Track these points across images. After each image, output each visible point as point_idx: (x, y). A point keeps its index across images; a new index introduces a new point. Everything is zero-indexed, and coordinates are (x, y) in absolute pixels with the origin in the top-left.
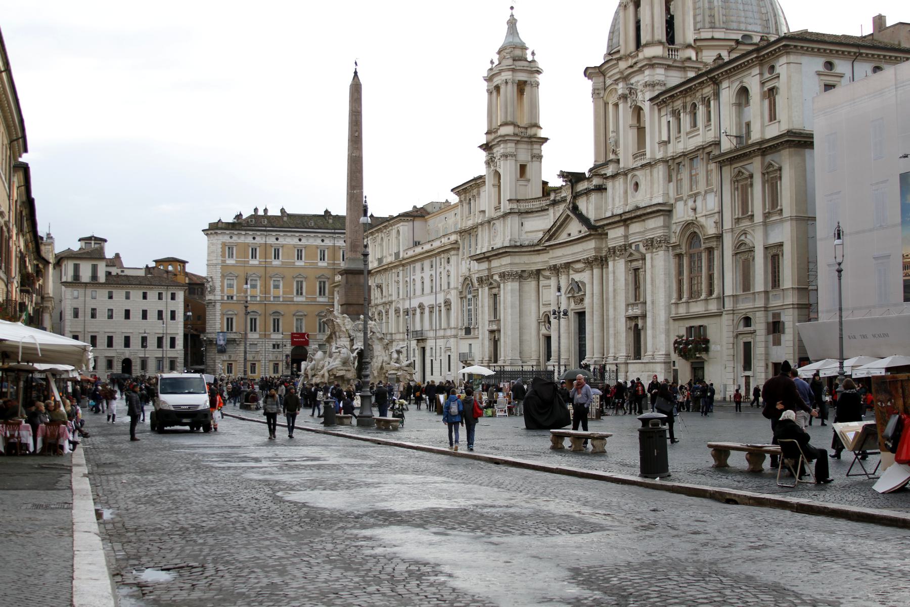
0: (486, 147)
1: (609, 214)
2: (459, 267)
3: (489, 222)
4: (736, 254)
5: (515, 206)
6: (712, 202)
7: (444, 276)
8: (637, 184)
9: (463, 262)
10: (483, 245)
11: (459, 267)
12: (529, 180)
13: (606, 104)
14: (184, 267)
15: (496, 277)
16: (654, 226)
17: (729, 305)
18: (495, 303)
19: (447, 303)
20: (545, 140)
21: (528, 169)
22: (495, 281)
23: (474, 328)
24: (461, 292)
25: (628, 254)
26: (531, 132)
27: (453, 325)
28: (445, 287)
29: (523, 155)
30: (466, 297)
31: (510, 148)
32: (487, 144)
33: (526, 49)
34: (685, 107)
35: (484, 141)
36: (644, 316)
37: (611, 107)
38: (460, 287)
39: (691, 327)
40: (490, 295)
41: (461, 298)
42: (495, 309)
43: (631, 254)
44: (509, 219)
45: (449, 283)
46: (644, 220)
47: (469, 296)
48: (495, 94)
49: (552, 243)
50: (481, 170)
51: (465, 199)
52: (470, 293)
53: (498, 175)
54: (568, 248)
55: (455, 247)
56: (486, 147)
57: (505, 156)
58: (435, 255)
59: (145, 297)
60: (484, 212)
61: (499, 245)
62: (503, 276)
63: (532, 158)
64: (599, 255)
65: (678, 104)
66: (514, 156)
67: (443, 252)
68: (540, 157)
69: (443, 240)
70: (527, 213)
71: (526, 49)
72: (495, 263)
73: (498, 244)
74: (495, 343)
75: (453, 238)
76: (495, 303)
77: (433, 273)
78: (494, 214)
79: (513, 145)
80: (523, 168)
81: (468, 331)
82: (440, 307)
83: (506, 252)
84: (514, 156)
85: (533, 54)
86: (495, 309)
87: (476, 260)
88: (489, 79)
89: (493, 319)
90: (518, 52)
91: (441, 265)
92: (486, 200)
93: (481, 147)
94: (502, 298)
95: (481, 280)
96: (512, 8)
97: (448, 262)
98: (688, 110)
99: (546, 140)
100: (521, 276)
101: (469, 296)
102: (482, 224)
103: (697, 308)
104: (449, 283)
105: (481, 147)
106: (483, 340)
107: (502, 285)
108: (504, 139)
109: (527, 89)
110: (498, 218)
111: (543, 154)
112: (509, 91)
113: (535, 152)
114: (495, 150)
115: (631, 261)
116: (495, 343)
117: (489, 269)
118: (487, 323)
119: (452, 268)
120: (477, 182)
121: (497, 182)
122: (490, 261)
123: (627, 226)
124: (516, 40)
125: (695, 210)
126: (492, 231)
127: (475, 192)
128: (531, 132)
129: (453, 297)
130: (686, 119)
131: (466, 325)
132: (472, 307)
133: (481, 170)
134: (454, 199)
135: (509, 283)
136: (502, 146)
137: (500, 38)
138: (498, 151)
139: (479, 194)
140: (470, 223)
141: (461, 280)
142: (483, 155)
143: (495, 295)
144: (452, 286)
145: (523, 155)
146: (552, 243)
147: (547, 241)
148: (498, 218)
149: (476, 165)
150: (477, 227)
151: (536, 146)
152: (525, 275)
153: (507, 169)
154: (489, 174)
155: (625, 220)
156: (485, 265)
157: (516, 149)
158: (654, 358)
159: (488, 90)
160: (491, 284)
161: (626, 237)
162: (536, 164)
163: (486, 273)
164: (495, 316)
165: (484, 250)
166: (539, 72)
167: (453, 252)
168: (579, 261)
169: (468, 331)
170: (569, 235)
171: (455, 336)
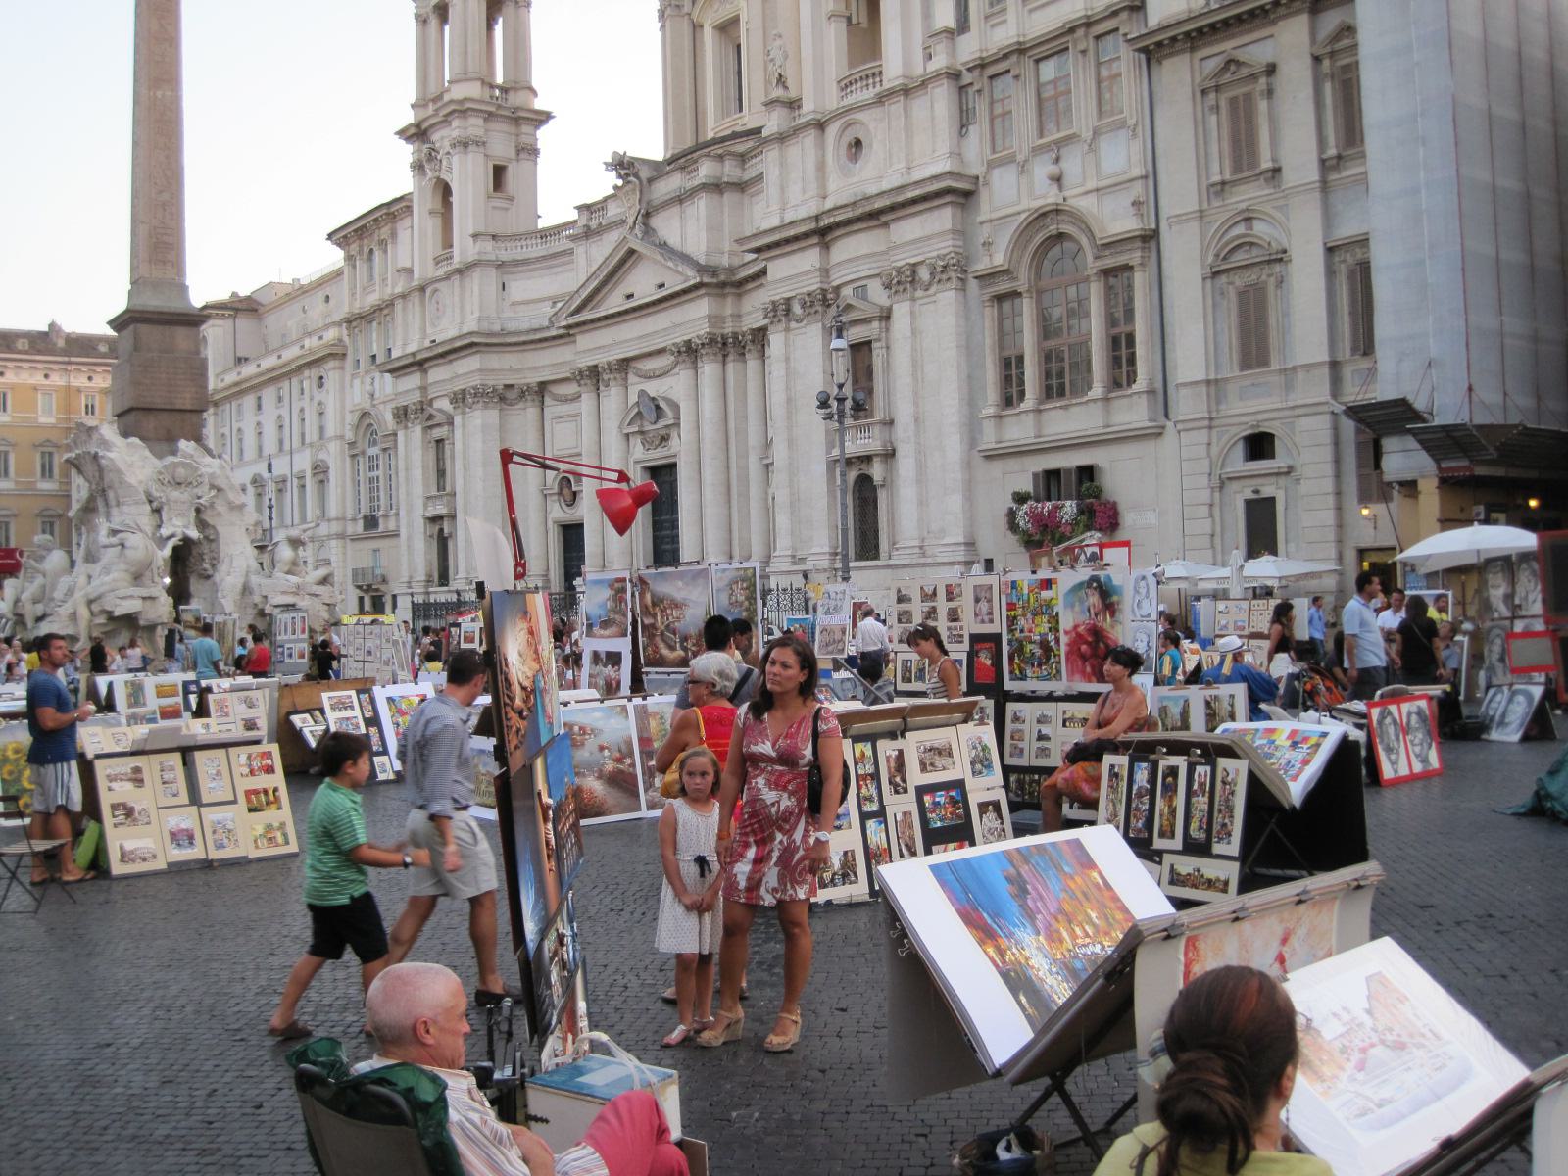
0: (416, 134)
1: (775, 222)
2: (347, 394)
3: (422, 289)
5: (488, 246)
7: (311, 417)
9: (357, 382)
10: (408, 337)
11: (347, 394)
12: (511, 199)
13: (697, 28)
15: (444, 404)
16: (924, 235)
18: (440, 459)
19: (320, 470)
22: (440, 410)
23: (385, 516)
24: (352, 444)
26: (515, 99)
27: (333, 510)
28: (312, 435)
29: (501, 146)
30: (363, 453)
31: (474, 126)
32: (418, 125)
35: (408, 118)
37: (708, 35)
38: (349, 435)
40: (425, 443)
41: (353, 456)
42: (441, 473)
44: (476, 275)
45: (322, 429)
47: (374, 451)
48: (434, 22)
51: (360, 252)
52: (374, 443)
53: (445, 191)
54: (625, 327)
55: (337, 354)
56: (416, 134)
57: (464, 145)
58: (288, 375)
60: (409, 271)
61: (452, 333)
63: (518, 152)
64: (718, 331)
66: (480, 143)
67: (309, 364)
68: (534, 152)
69: (307, 343)
70: (516, 263)
72: (437, 373)
73: (447, 330)
74: (443, 543)
75: (331, 335)
76: (440, 459)
77: (285, 412)
78: (433, 272)
79: (480, 121)
80: (499, 172)
81: (371, 522)
82: (301, 478)
83: (472, 345)
84: (480, 143)
86: (441, 473)
89: (434, 492)
91: (301, 394)
92: (413, 247)
93: (398, 133)
94: (458, 446)
95: (402, 415)
97: (321, 385)
100: (504, 396)
101: (374, 451)
102: (403, 296)
104: (322, 429)
105: (398, 133)
106: (409, 538)
107: (458, 420)
108: (462, 110)
110: (447, 277)
111: (540, 145)
113: (524, 139)
114: (435, 137)
116: (443, 543)
117: (424, 389)
118: (420, 503)
119: (330, 397)
120: (392, 212)
121: (438, 206)
122: (425, 372)
123: (826, 247)
126: (430, 307)
127: (385, 232)
128: (515, 99)
129: (334, 456)
131: (365, 510)
132: (380, 473)
135: (478, 413)
136: (456, 123)
138: (442, 138)
139: (394, 235)
140: (373, 299)
141: (351, 419)
142: (406, 152)
143: (439, 442)
144: (330, 431)
145: (501, 146)
147: (572, 314)
148: (447, 277)
149: (392, 174)
150: (390, 304)
151: (525, 129)
152: (512, 395)
153: (467, 176)
154: (421, 189)
155: (823, 233)
156: (413, 381)
157: (487, 131)
159: (417, 17)
160: (431, 417)
161: (825, 272)
162: (526, 165)
163: (417, 397)
164: (441, 487)
165: (411, 349)
167: (331, 364)
169: (371, 522)
170: (630, 296)
171: (341, 536)
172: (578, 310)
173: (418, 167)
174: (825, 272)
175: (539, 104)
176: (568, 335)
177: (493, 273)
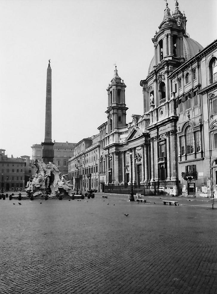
0: (108, 112)
4: (211, 132)
6: (197, 111)
8: (162, 112)
12: (121, 122)
14: (29, 158)
17: (207, 154)
20: (127, 108)
21: (121, 118)
25: (159, 139)
33: (121, 79)
34: (183, 76)
36: (166, 163)
39: (187, 166)
43: (160, 139)
46: (165, 125)
49: (128, 141)
50: (106, 120)
55: (99, 146)
59: (13, 166)
62: (113, 153)
65: (180, 75)
71: (121, 79)
85: (123, 81)
87: (104, 149)
88: (108, 90)
90: (118, 81)
95: (106, 156)
96: (116, 67)
98: (185, 77)
99: (127, 108)
103: (191, 157)
108: (113, 108)
109: (121, 92)
112: (114, 94)
115: (160, 142)
120: (105, 125)
124: (117, 77)
125: (189, 116)
127: (104, 127)
128: (123, 106)
130: (183, 81)
133: (106, 120)
134: (98, 132)
137: (113, 76)
138: (111, 112)
142: (107, 115)
146: (128, 141)
153: (114, 118)
154: (109, 121)
158: (170, 180)
162: (124, 117)
166: (125, 86)
168: (139, 146)
170: (135, 137)
172: (128, 140)
173: (108, 117)
174: (158, 133)
175: (126, 107)
176: (127, 144)
177: (117, 134)
